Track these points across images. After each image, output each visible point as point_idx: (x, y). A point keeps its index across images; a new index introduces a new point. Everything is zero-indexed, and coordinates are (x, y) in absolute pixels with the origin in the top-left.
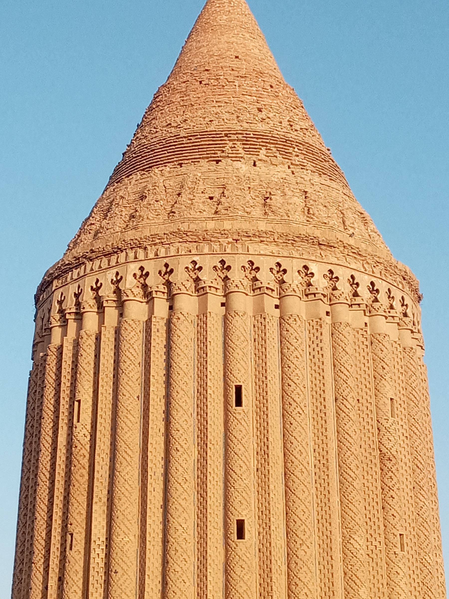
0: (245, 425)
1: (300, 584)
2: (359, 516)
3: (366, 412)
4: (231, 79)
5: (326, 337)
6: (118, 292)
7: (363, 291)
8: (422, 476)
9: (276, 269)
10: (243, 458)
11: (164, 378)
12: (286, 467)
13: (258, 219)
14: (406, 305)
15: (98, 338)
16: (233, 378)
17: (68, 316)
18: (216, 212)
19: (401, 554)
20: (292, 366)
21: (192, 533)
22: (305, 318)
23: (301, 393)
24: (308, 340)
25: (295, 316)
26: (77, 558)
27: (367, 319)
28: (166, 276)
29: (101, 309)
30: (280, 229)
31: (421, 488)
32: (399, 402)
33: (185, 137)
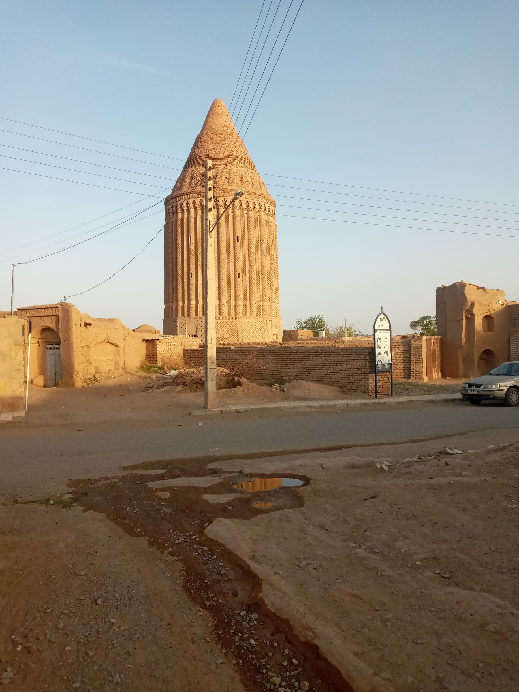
7: (267, 209)
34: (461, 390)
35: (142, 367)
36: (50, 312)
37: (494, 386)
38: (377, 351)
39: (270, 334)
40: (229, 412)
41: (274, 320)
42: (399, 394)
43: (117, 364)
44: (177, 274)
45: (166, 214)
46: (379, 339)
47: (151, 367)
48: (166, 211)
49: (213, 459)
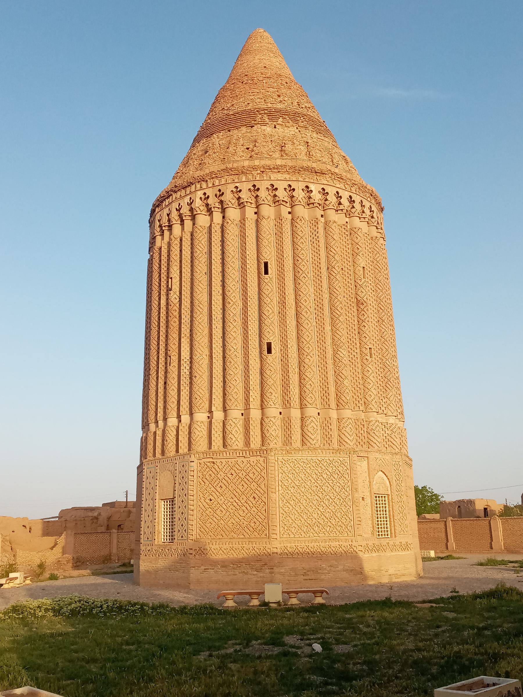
0: (271, 286)
1: (307, 379)
2: (343, 337)
3: (347, 275)
4: (261, 79)
5: (321, 230)
6: (191, 210)
8: (383, 314)
9: (288, 189)
10: (270, 306)
11: (221, 261)
12: (296, 310)
13: (276, 159)
14: (373, 211)
15: (181, 240)
16: (262, 258)
17: (164, 228)
18: (251, 157)
19: (370, 359)
20: (300, 249)
21: (240, 352)
22: (307, 219)
23: (305, 265)
24: (310, 232)
25: (300, 218)
26: (174, 370)
27: (347, 220)
28: (220, 198)
29: (182, 221)
30: (290, 163)
31: (383, 321)
32: (369, 269)
33: (232, 115)
41: (372, 456)
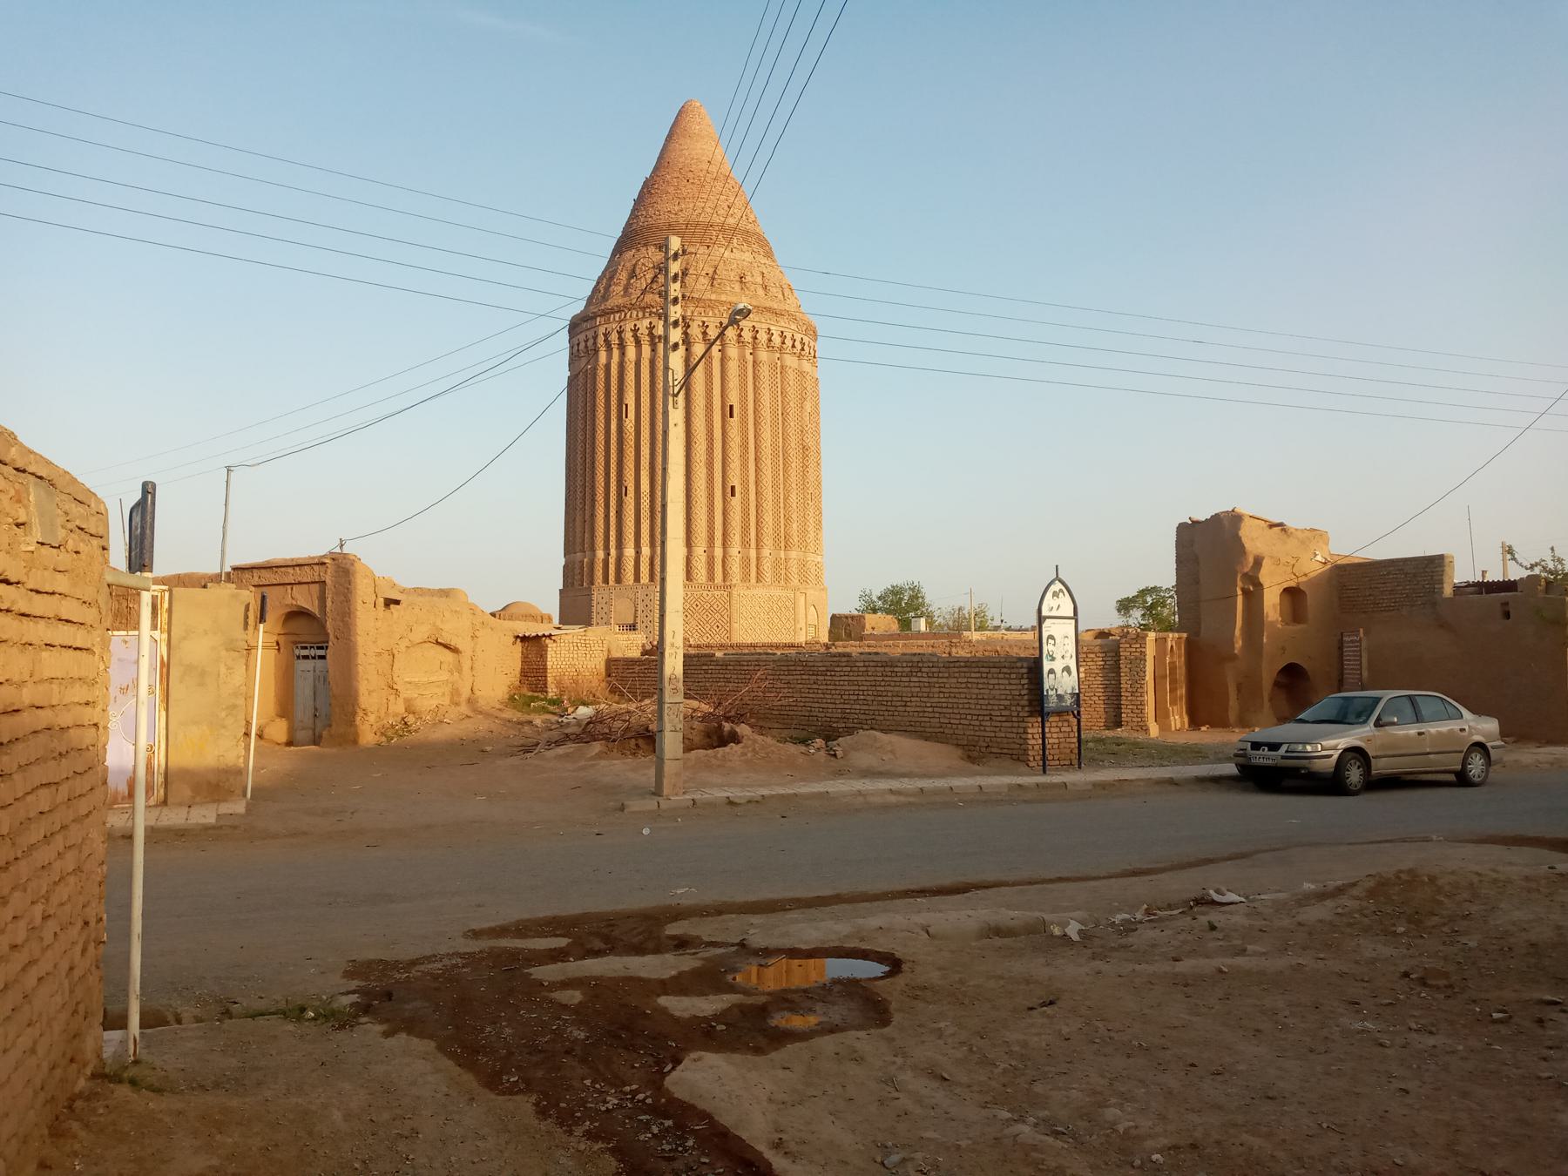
7: (798, 344)
34: (1236, 755)
35: (512, 698)
36: (307, 574)
37: (1309, 748)
38: (1047, 665)
39: (802, 624)
40: (711, 805)
42: (1096, 763)
43: (455, 692)
44: (593, 487)
45: (571, 354)
46: (1051, 637)
47: (533, 699)
48: (572, 347)
49: (678, 914)
